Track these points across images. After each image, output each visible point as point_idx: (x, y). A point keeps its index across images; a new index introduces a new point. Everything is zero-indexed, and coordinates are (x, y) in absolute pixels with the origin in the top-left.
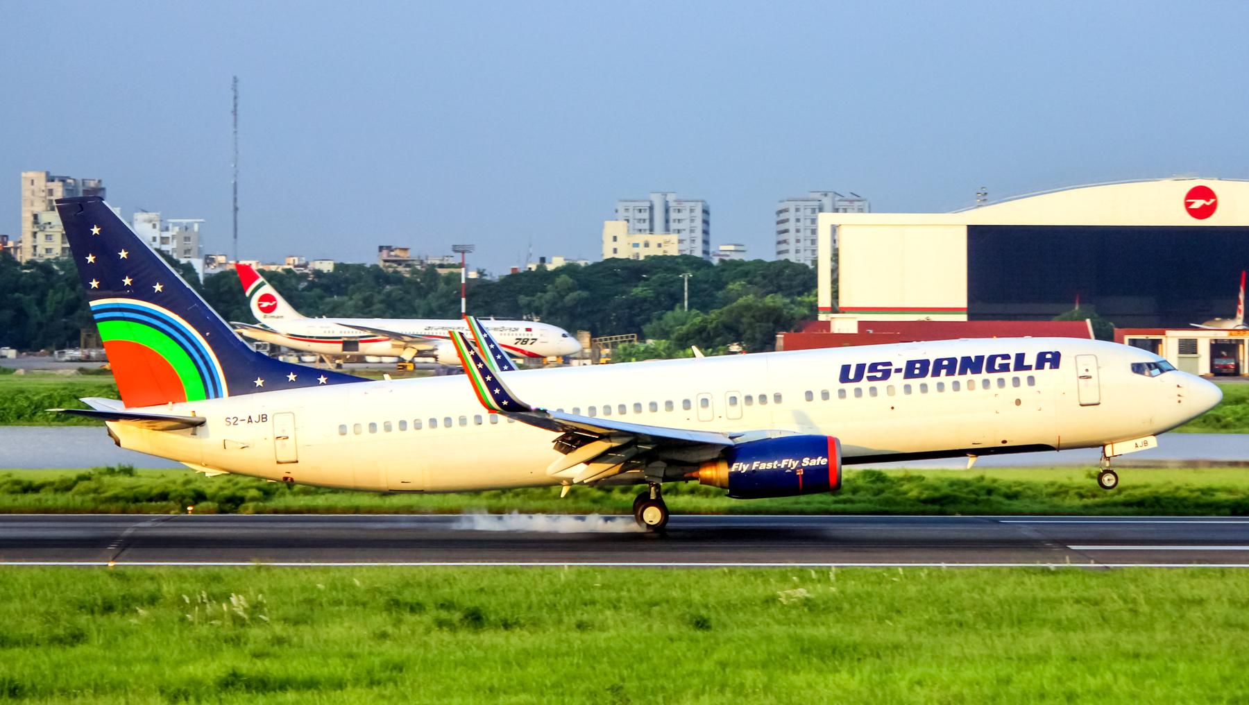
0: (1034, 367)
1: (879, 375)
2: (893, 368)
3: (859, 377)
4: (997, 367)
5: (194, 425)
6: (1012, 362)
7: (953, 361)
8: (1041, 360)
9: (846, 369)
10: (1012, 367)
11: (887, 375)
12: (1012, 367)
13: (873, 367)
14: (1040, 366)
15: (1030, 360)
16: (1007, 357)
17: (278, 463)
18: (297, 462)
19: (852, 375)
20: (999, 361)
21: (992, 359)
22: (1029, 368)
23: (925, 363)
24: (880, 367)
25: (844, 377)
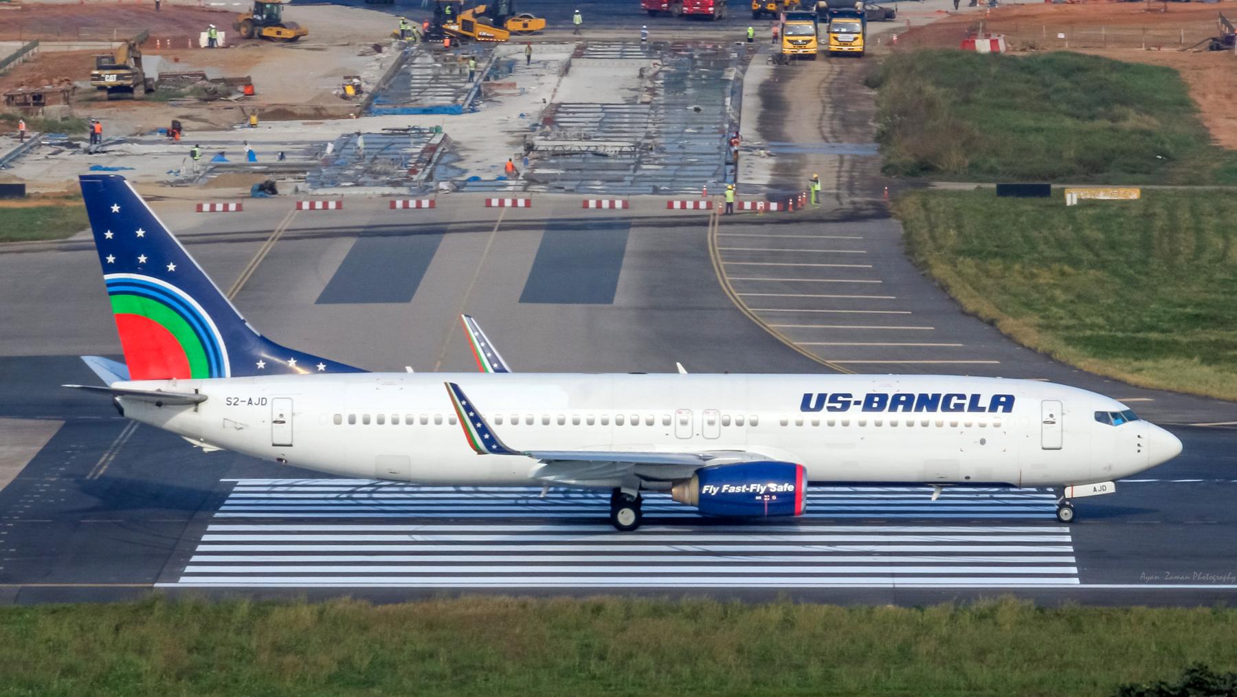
0: (987, 409)
1: (839, 406)
2: (852, 400)
3: (819, 405)
4: (952, 407)
5: (195, 402)
6: (967, 402)
7: (910, 397)
8: (995, 402)
9: (807, 398)
10: (966, 407)
11: (846, 406)
12: (966, 407)
13: (834, 398)
14: (993, 408)
15: (985, 402)
16: (962, 397)
17: (274, 445)
18: (291, 445)
19: (813, 404)
20: (955, 400)
21: (948, 398)
22: (983, 409)
23: (883, 398)
24: (840, 398)
25: (805, 405)
